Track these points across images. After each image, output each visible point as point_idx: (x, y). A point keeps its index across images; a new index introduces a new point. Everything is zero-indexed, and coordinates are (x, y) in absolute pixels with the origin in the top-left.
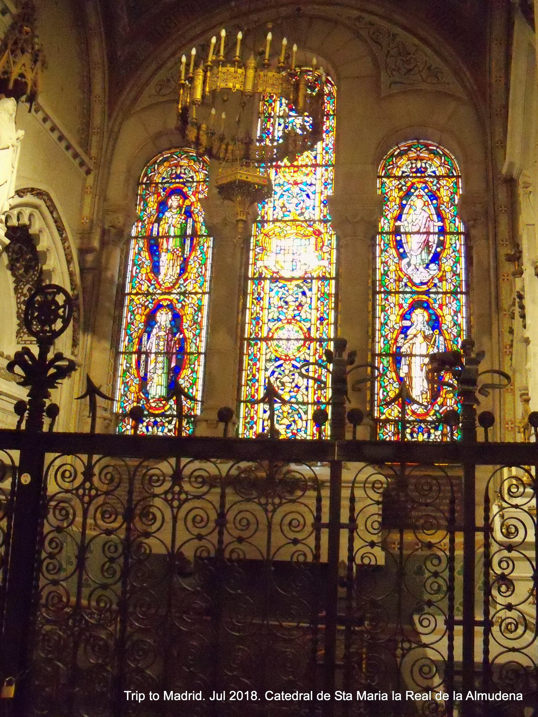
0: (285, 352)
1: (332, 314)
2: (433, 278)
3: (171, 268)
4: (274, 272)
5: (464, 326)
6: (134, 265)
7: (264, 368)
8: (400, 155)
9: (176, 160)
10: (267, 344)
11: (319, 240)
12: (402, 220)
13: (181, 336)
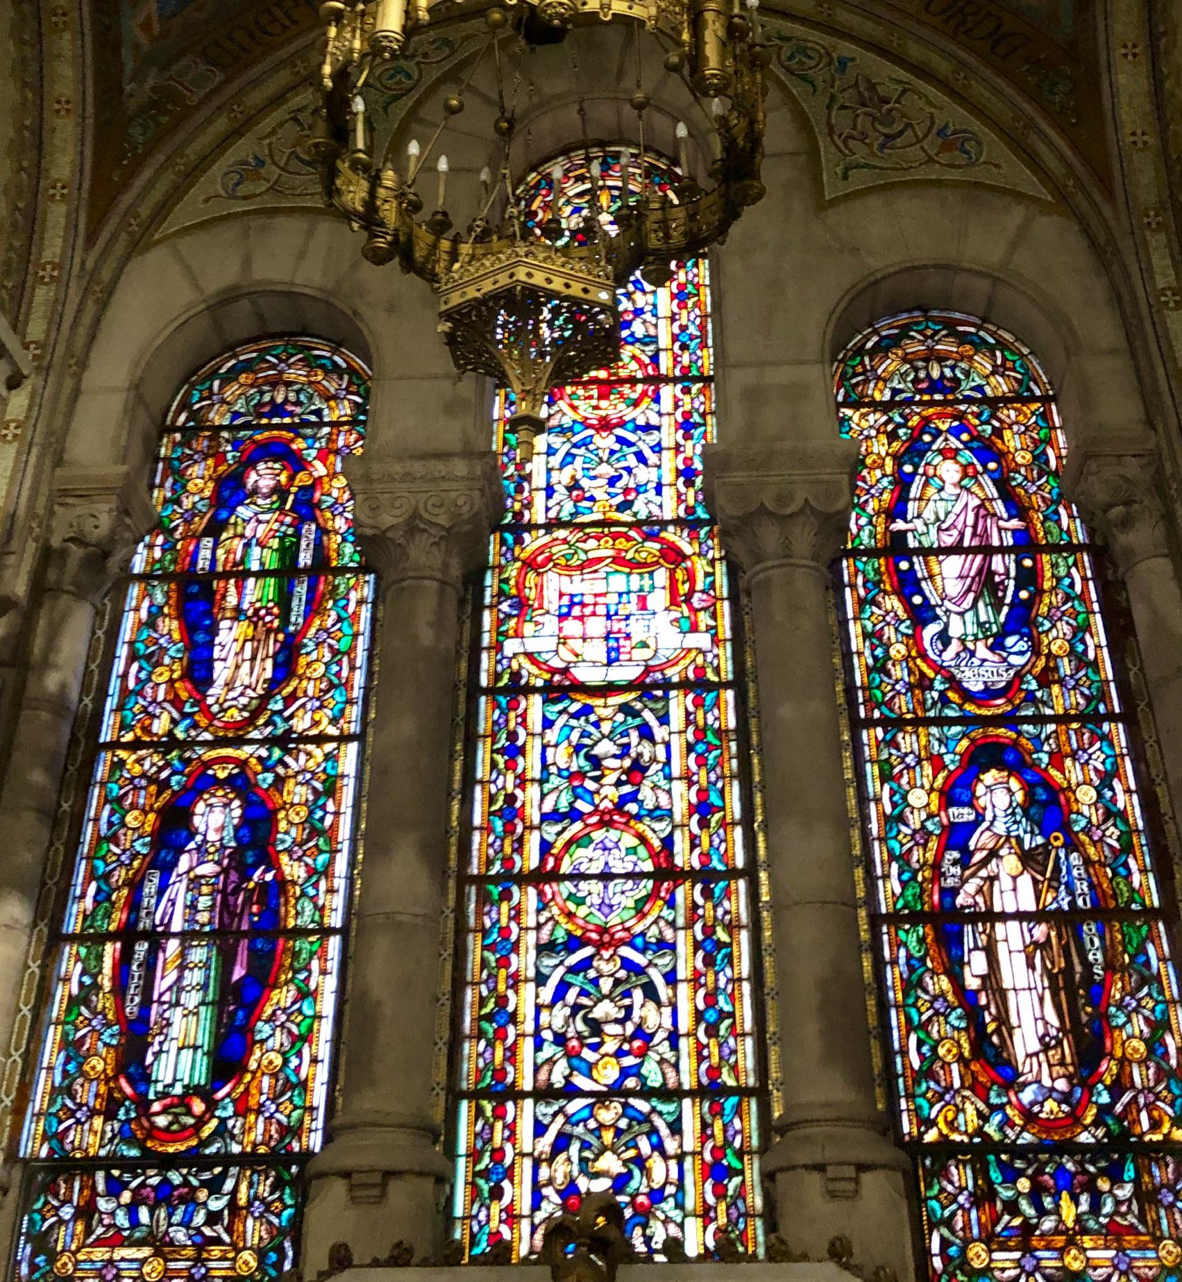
0: (598, 919)
1: (734, 792)
2: (1019, 676)
3: (246, 667)
4: (553, 671)
5: (1137, 817)
6: (133, 657)
7: (531, 973)
8: (882, 349)
9: (274, 367)
10: (541, 894)
11: (680, 575)
12: (909, 517)
13: (269, 877)
